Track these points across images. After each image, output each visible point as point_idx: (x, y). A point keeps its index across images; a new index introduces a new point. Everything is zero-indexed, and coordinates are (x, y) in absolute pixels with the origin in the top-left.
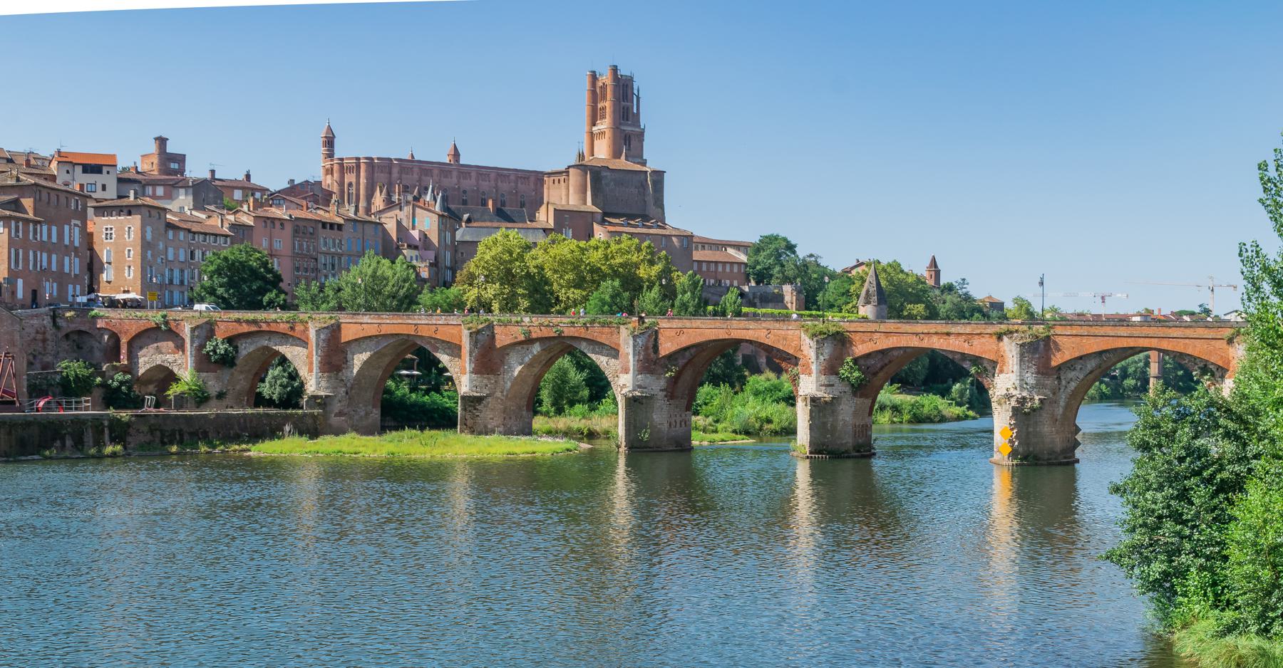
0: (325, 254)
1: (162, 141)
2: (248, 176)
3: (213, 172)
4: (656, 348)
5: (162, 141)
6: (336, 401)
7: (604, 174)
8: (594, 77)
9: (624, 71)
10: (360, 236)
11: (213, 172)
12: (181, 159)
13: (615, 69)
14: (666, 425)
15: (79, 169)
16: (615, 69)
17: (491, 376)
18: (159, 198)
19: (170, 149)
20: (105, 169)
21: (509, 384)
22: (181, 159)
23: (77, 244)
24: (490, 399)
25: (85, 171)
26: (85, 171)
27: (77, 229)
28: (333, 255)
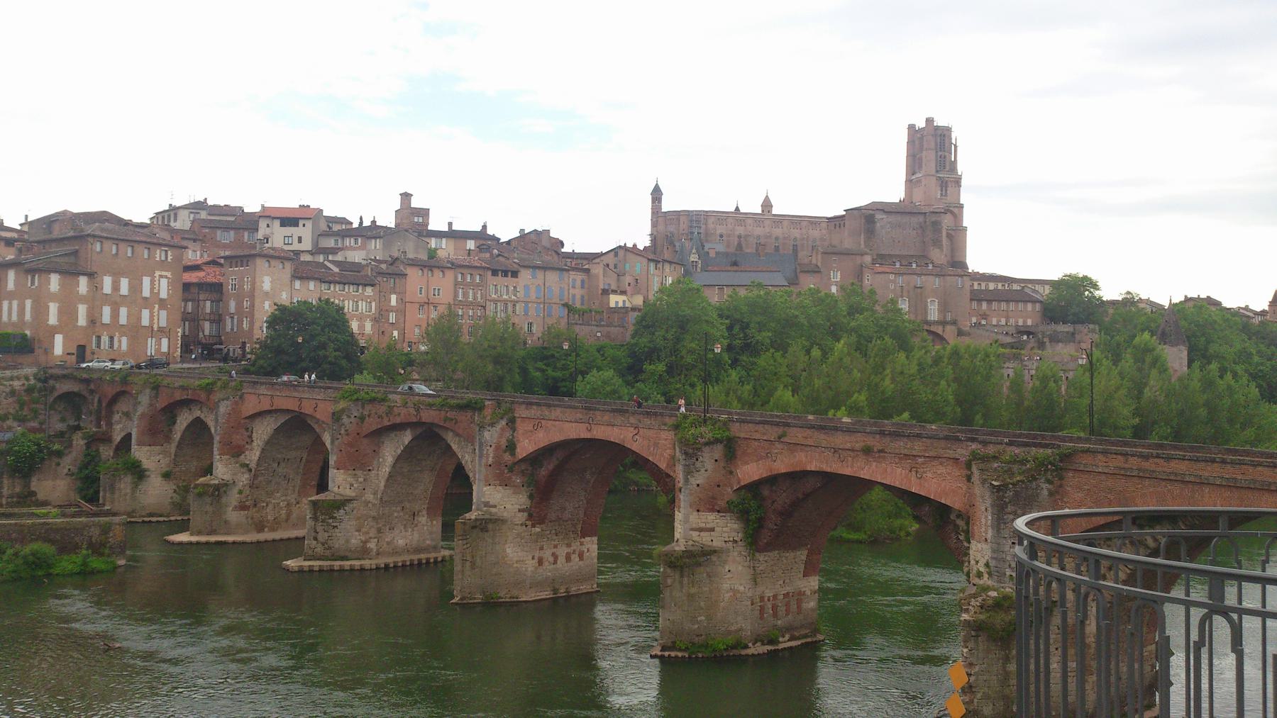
0: (495, 302)
1: (406, 197)
2: (485, 227)
3: (450, 224)
4: (511, 447)
5: (406, 197)
6: (235, 491)
7: (879, 216)
8: (911, 128)
9: (940, 122)
10: (541, 282)
11: (450, 224)
12: (424, 213)
13: (929, 121)
14: (531, 564)
15: (277, 223)
16: (929, 121)
17: (359, 473)
18: (355, 249)
19: (415, 203)
20: (301, 223)
21: (383, 484)
22: (424, 213)
23: (164, 295)
24: (355, 504)
25: (282, 225)
26: (282, 225)
27: (164, 282)
28: (506, 303)
